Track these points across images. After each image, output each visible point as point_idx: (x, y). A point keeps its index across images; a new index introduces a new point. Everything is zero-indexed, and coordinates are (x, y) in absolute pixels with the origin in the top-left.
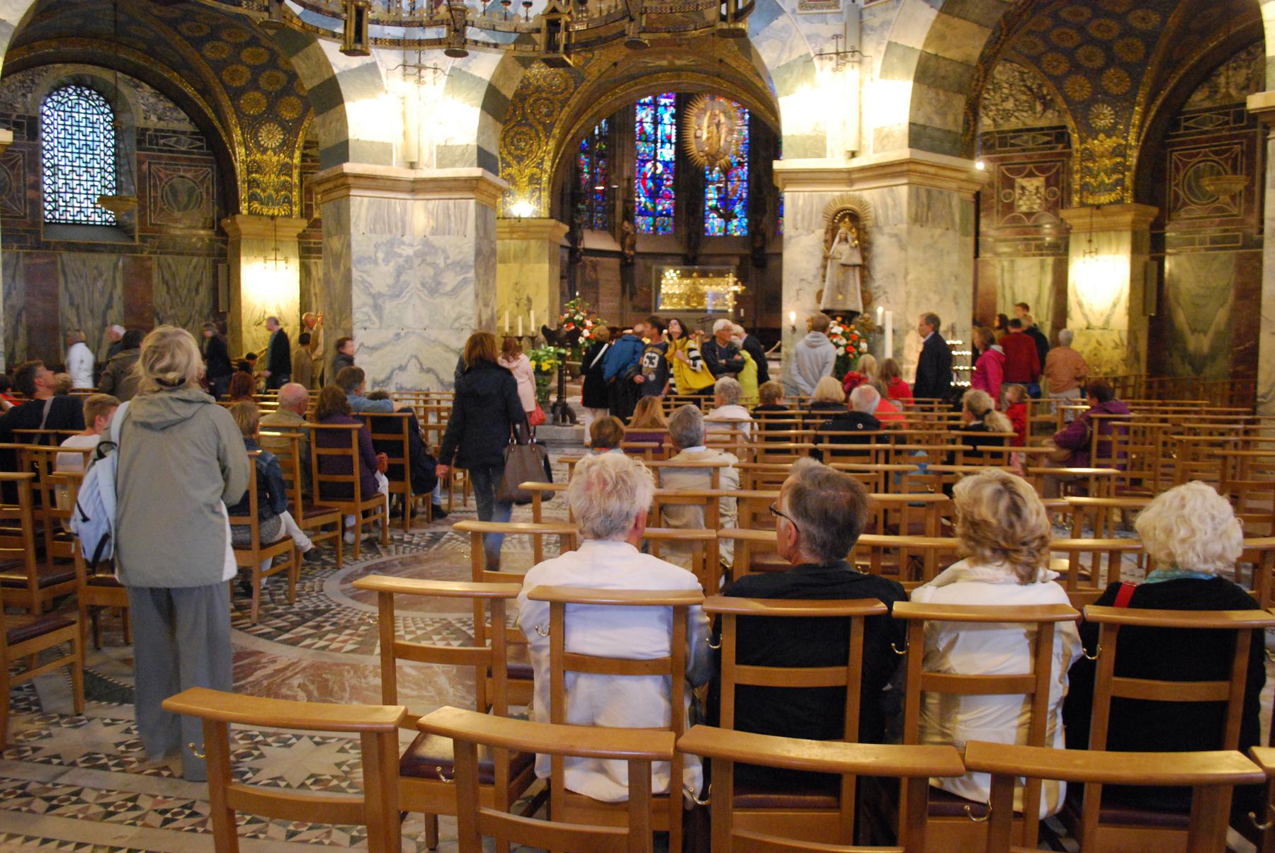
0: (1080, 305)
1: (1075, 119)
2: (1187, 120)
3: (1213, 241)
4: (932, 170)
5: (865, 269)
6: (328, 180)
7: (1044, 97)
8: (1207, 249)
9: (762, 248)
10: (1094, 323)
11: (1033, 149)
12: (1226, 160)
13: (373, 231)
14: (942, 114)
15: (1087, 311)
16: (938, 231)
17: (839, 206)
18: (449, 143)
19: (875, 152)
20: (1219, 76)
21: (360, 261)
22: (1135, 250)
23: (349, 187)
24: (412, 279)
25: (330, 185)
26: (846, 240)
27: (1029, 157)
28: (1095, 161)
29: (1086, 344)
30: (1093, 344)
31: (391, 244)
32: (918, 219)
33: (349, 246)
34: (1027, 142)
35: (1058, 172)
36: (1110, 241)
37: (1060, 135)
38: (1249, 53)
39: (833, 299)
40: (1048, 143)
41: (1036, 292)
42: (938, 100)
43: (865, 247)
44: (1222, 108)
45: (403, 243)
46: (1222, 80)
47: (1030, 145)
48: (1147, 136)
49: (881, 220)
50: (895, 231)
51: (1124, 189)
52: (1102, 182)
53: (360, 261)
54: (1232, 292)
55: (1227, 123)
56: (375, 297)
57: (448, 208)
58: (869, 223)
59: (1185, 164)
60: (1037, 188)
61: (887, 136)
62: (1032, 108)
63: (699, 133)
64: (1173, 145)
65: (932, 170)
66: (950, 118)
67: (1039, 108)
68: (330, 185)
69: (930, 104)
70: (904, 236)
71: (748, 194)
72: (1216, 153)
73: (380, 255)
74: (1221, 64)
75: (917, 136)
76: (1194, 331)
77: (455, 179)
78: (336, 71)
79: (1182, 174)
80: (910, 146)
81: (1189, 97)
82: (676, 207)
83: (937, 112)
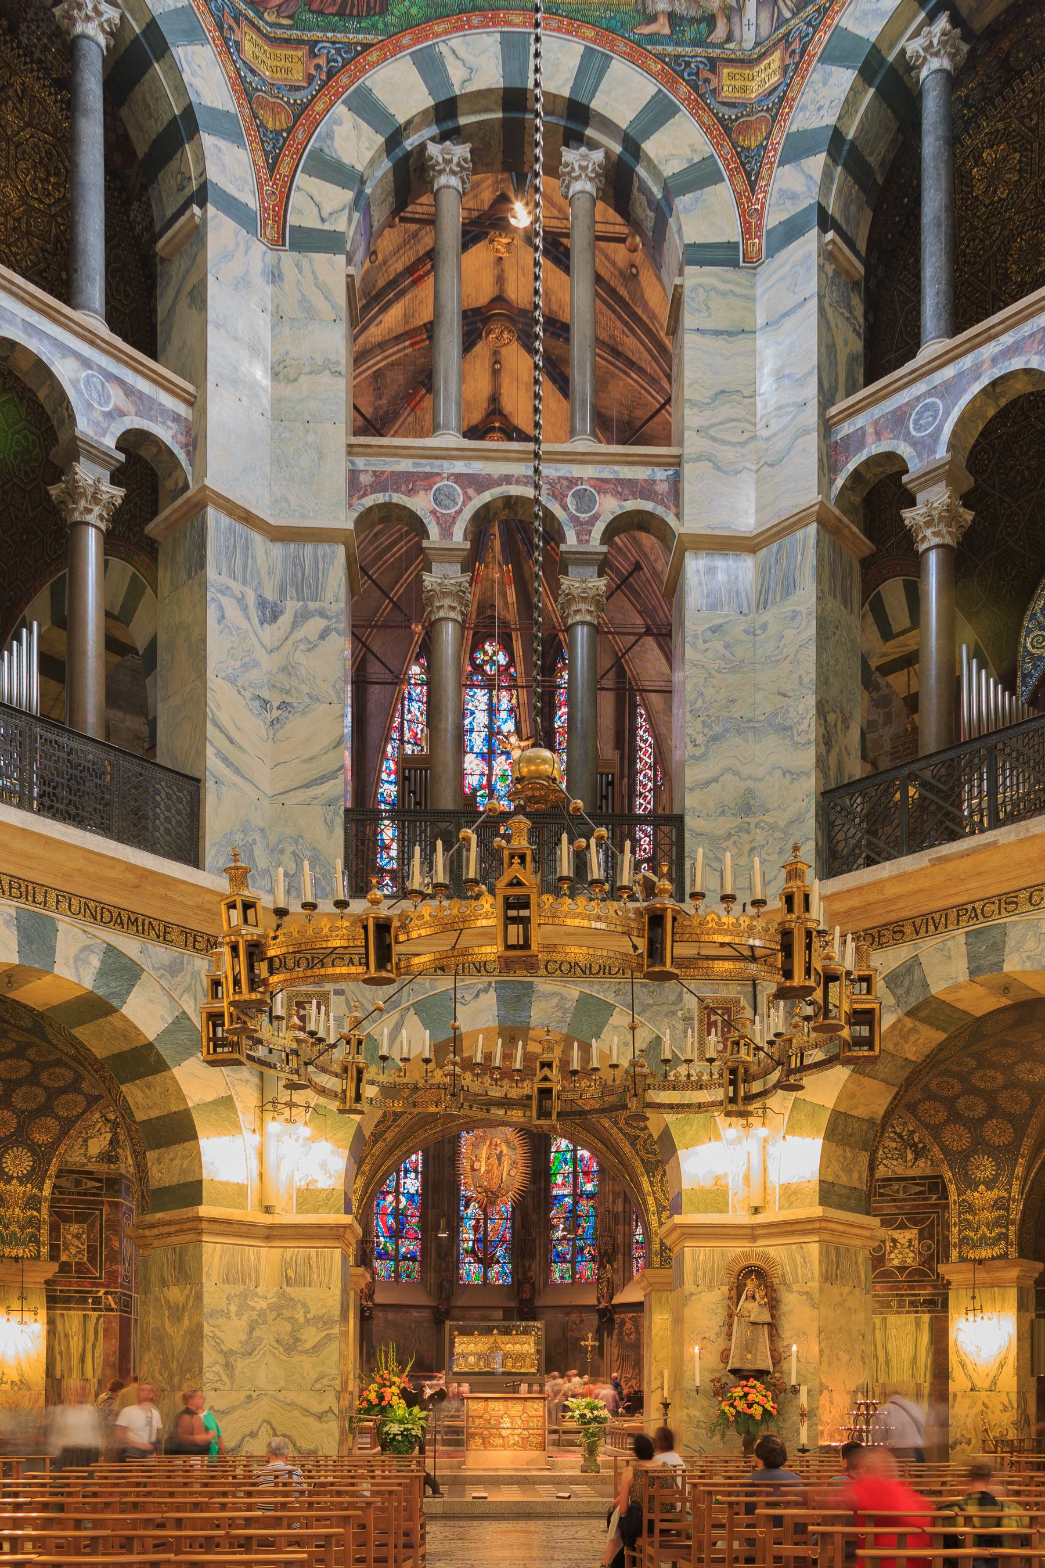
4: (841, 1228)
5: (773, 1327)
14: (849, 1171)
17: (745, 1263)
24: (266, 1335)
26: (754, 1298)
32: (828, 1277)
39: (742, 1359)
42: (845, 1157)
43: (773, 1305)
49: (789, 1278)
58: (776, 1281)
65: (841, 1228)
66: (856, 1175)
69: (838, 1161)
80: (820, 1204)
83: (844, 1170)
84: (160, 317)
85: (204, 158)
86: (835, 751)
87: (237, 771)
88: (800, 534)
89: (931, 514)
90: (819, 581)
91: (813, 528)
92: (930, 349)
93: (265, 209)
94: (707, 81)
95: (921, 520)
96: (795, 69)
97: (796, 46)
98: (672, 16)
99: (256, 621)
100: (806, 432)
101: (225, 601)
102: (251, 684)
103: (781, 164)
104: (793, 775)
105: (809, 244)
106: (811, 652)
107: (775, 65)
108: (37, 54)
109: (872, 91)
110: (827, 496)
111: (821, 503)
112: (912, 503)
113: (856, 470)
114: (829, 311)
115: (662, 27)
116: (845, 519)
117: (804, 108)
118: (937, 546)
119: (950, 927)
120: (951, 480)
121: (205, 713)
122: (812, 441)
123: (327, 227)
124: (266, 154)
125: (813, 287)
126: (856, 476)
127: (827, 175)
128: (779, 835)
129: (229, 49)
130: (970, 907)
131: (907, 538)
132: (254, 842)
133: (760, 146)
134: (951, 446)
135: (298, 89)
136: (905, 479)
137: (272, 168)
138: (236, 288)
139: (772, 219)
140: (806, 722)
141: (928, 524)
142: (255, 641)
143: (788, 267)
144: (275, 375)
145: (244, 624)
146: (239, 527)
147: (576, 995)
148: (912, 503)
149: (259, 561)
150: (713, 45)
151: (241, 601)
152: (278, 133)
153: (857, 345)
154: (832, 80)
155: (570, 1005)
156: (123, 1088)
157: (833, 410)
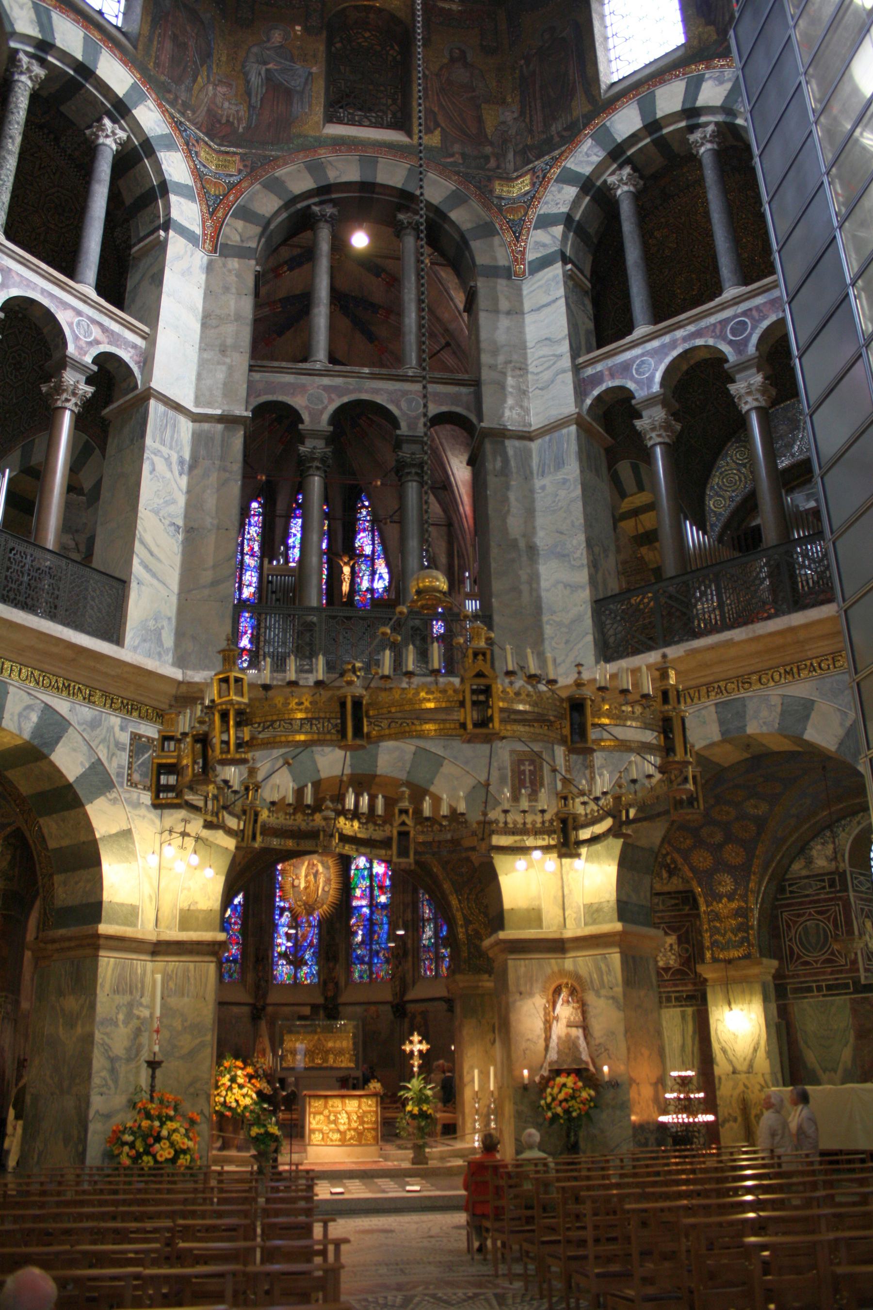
0: (724, 1051)
1: (700, 885)
2: (790, 885)
3: (829, 988)
6: (70, 939)
7: (667, 866)
8: (824, 996)
9: (335, 997)
10: (739, 1067)
11: (663, 911)
12: (828, 919)
13: (116, 991)
15: (732, 1057)
16: (642, 993)
18: (192, 908)
19: (586, 924)
20: (811, 849)
21: (102, 1023)
22: (766, 1000)
23: (97, 948)
25: (73, 944)
27: (662, 918)
28: (721, 922)
29: (734, 1088)
30: (741, 1088)
31: (130, 1005)
33: (92, 1006)
34: (658, 904)
35: (687, 931)
36: (743, 992)
37: (688, 898)
38: (832, 831)
40: (676, 905)
41: (680, 1043)
44: (817, 875)
45: (141, 1005)
46: (814, 853)
47: (661, 907)
48: (763, 899)
50: (611, 993)
51: (750, 945)
52: (730, 940)
53: (102, 1023)
54: (852, 1032)
55: (824, 888)
56: (112, 1060)
57: (188, 970)
59: (795, 922)
60: (671, 945)
61: (598, 910)
62: (659, 875)
63: (296, 883)
64: (782, 906)
67: (665, 875)
68: (67, 944)
70: (620, 997)
71: (320, 940)
72: (818, 913)
73: (121, 1017)
74: (813, 839)
75: (624, 908)
76: (825, 1070)
77: (199, 943)
78: (98, 836)
79: (793, 931)
81: (790, 866)
82: (244, 952)
84: (128, 289)
85: (169, 207)
86: (600, 575)
87: (154, 575)
88: (565, 431)
89: (652, 423)
90: (581, 460)
91: (573, 428)
92: (640, 331)
93: (204, 234)
94: (486, 186)
95: (648, 427)
96: (541, 181)
97: (541, 175)
98: (463, 155)
99: (177, 473)
100: (564, 371)
101: (157, 460)
102: (169, 515)
103: (535, 228)
104: (573, 588)
105: (557, 270)
106: (579, 505)
107: (527, 182)
108: (69, 152)
109: (588, 199)
110: (581, 409)
111: (578, 414)
112: (640, 417)
113: (599, 395)
114: (572, 305)
115: (458, 158)
116: (594, 424)
117: (546, 203)
118: (660, 443)
119: (703, 700)
120: (665, 404)
121: (134, 535)
122: (569, 377)
123: (245, 245)
124: (209, 206)
125: (561, 291)
126: (599, 398)
127: (565, 236)
128: (564, 630)
129: (190, 154)
130: (716, 685)
131: (638, 437)
132: (163, 627)
133: (521, 219)
134: (662, 385)
135: (231, 176)
136: (633, 402)
137: (212, 214)
138: (183, 274)
139: (530, 256)
140: (579, 552)
141: (653, 429)
142: (175, 486)
143: (543, 282)
145: (168, 475)
146: (171, 413)
147: (413, 748)
148: (640, 417)
149: (182, 434)
150: (488, 170)
151: (168, 460)
152: (217, 197)
153: (591, 325)
154: (564, 191)
155: (409, 757)
156: (41, 821)
157: (581, 360)
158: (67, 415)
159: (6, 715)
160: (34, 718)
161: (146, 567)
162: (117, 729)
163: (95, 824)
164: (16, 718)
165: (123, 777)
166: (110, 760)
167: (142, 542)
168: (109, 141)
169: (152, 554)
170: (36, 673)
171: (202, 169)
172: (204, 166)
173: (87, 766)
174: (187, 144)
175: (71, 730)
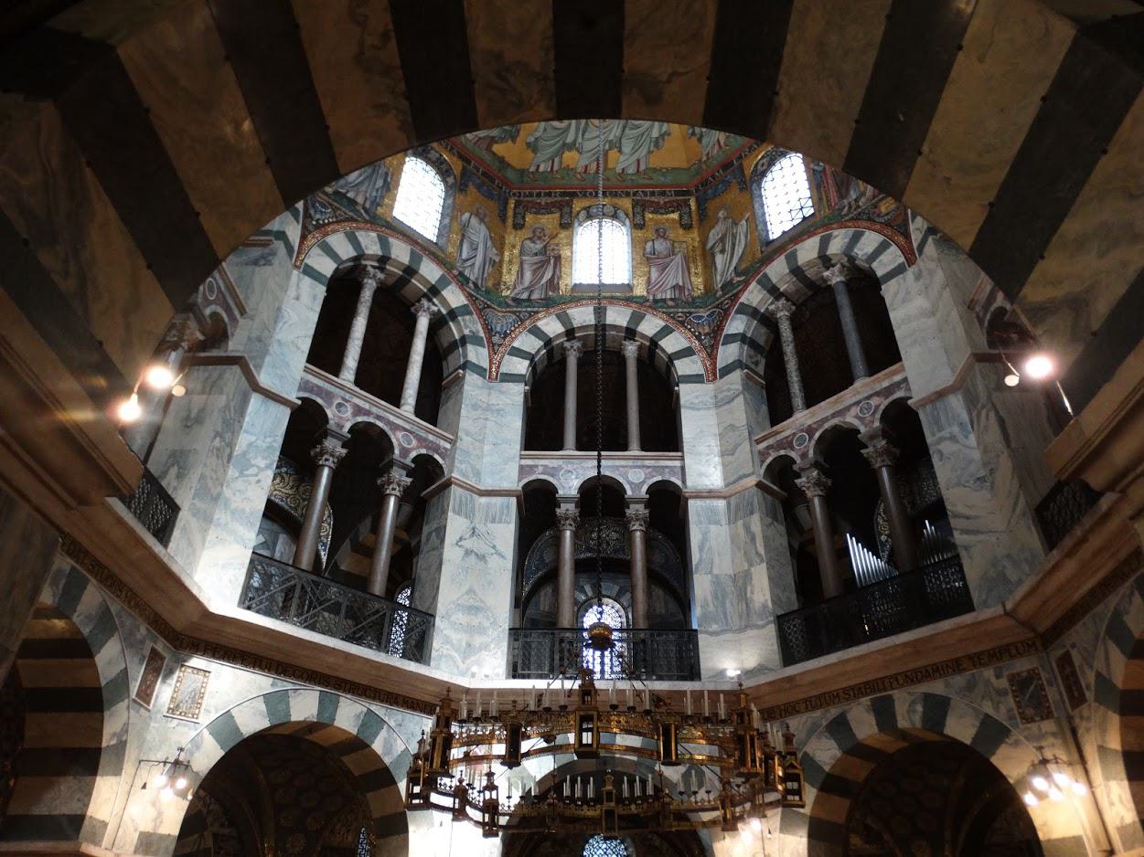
78: (1011, 781)
87: (977, 532)
144: (933, 314)
158: (884, 470)
159: (899, 718)
160: (919, 708)
161: (967, 532)
162: (993, 679)
163: (1005, 772)
164: (906, 715)
165: (1015, 718)
166: (997, 708)
167: (957, 516)
168: (834, 282)
169: (968, 518)
170: (909, 674)
171: (886, 218)
172: (888, 214)
173: (978, 724)
174: (869, 219)
175: (952, 703)
